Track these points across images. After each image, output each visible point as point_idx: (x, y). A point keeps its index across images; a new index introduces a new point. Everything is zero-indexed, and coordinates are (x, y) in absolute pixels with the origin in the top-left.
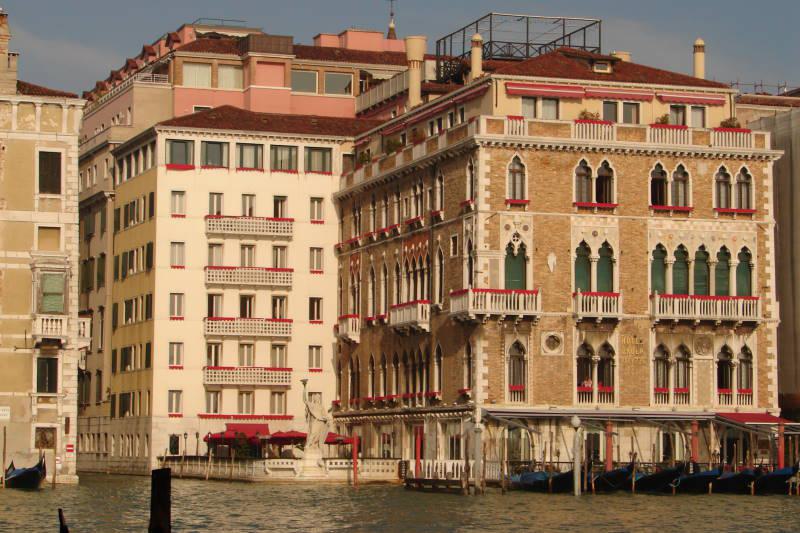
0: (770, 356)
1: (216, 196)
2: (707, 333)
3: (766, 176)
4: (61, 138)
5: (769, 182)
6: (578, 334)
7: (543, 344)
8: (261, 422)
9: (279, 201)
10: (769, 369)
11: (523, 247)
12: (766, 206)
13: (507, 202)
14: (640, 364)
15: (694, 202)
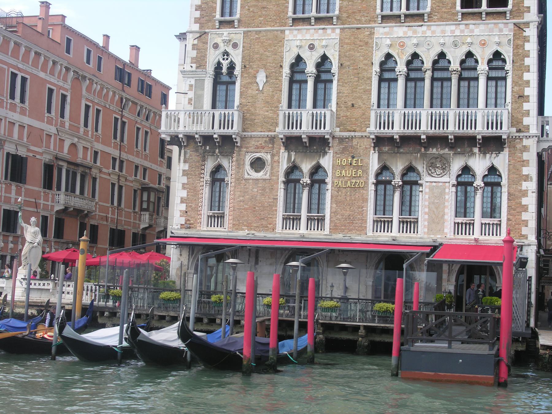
0: (527, 178)
2: (442, 152)
6: (286, 154)
7: (248, 167)
10: (525, 194)
11: (232, 67)
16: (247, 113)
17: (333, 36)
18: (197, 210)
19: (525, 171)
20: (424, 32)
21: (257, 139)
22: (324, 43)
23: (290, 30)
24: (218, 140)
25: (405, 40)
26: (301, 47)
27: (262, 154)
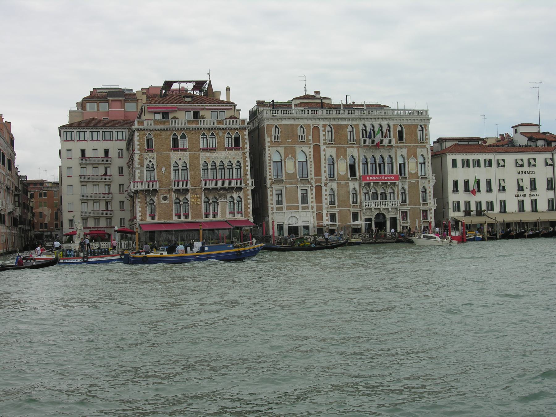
0: (249, 199)
1: (83, 152)
3: (245, 135)
5: (247, 137)
7: (161, 199)
8: (103, 229)
9: (107, 152)
12: (246, 146)
18: (145, 215)
19: (248, 197)
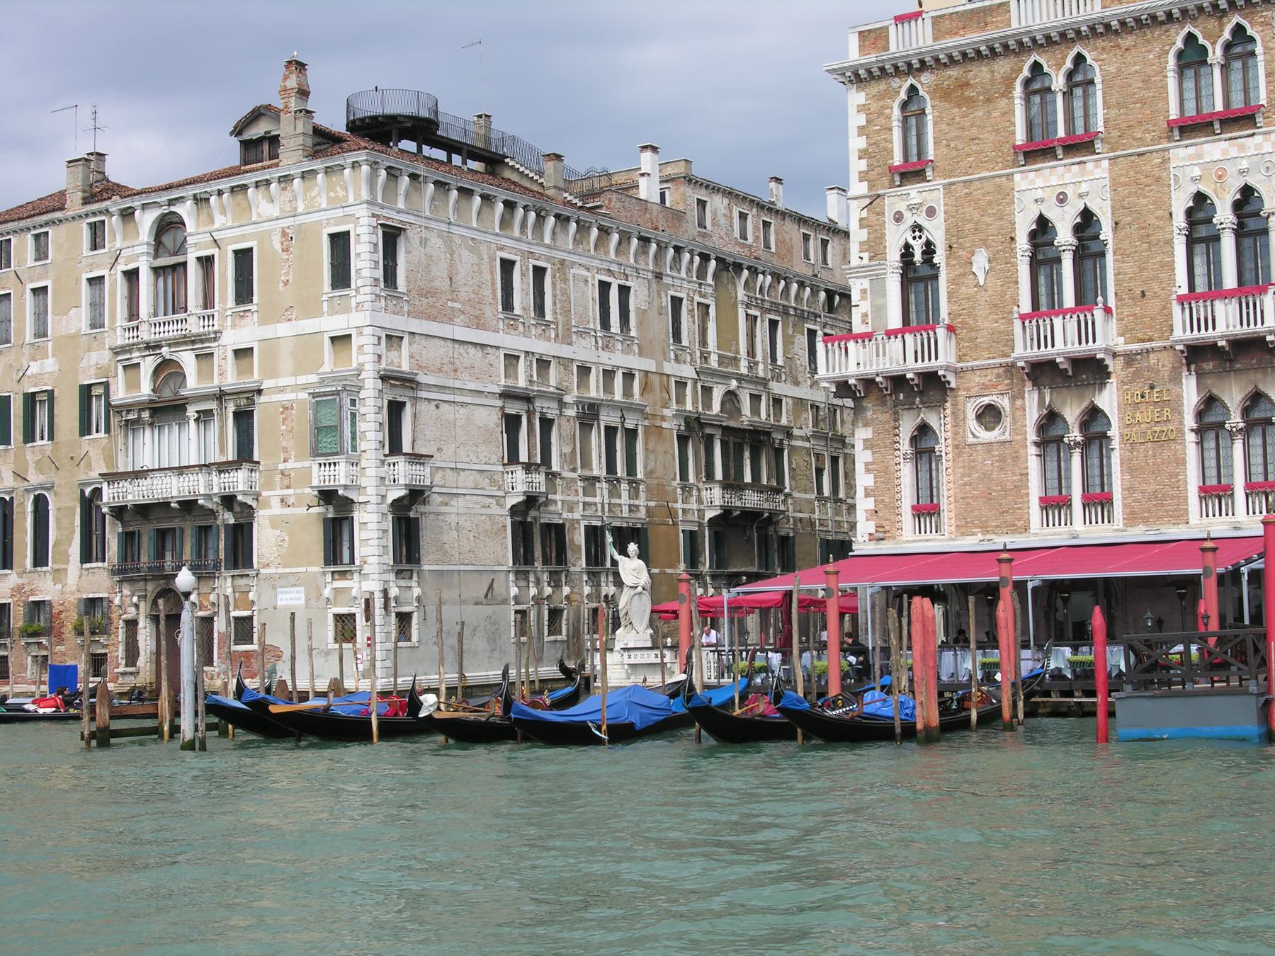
4: (348, 211)
7: (972, 423)
11: (929, 249)
13: (892, 169)
14: (1166, 440)
15: (1269, 92)
16: (962, 328)
17: (1098, 173)
18: (895, 509)
20: (1258, 146)
21: (984, 372)
22: (1084, 188)
23: (1021, 172)
24: (916, 381)
25: (1226, 166)
26: (1042, 200)
27: (994, 398)
